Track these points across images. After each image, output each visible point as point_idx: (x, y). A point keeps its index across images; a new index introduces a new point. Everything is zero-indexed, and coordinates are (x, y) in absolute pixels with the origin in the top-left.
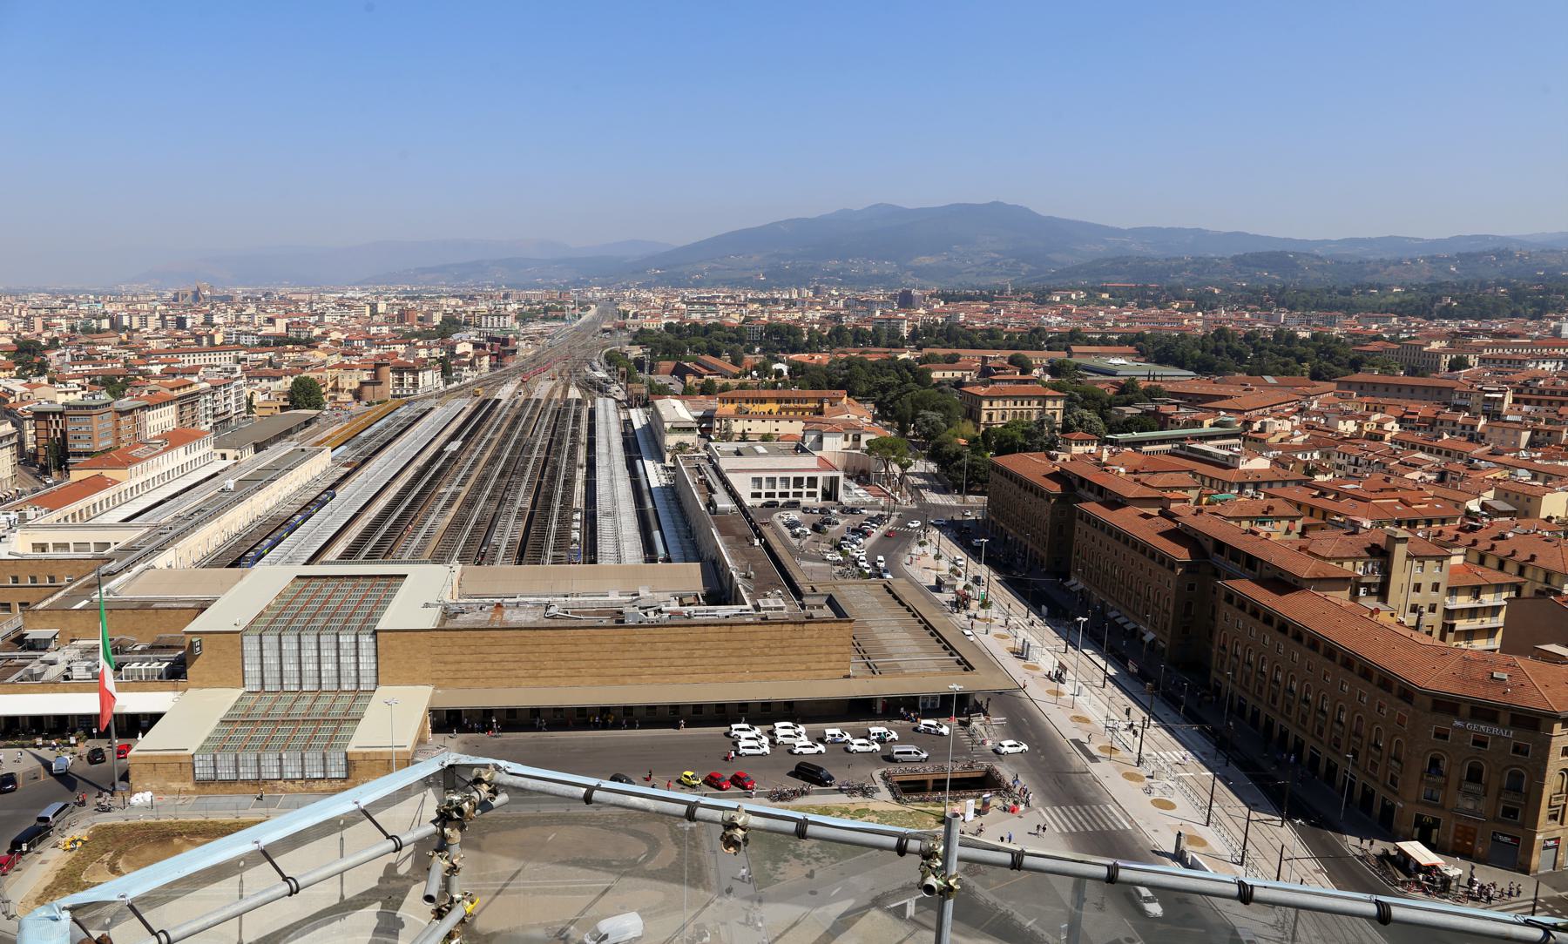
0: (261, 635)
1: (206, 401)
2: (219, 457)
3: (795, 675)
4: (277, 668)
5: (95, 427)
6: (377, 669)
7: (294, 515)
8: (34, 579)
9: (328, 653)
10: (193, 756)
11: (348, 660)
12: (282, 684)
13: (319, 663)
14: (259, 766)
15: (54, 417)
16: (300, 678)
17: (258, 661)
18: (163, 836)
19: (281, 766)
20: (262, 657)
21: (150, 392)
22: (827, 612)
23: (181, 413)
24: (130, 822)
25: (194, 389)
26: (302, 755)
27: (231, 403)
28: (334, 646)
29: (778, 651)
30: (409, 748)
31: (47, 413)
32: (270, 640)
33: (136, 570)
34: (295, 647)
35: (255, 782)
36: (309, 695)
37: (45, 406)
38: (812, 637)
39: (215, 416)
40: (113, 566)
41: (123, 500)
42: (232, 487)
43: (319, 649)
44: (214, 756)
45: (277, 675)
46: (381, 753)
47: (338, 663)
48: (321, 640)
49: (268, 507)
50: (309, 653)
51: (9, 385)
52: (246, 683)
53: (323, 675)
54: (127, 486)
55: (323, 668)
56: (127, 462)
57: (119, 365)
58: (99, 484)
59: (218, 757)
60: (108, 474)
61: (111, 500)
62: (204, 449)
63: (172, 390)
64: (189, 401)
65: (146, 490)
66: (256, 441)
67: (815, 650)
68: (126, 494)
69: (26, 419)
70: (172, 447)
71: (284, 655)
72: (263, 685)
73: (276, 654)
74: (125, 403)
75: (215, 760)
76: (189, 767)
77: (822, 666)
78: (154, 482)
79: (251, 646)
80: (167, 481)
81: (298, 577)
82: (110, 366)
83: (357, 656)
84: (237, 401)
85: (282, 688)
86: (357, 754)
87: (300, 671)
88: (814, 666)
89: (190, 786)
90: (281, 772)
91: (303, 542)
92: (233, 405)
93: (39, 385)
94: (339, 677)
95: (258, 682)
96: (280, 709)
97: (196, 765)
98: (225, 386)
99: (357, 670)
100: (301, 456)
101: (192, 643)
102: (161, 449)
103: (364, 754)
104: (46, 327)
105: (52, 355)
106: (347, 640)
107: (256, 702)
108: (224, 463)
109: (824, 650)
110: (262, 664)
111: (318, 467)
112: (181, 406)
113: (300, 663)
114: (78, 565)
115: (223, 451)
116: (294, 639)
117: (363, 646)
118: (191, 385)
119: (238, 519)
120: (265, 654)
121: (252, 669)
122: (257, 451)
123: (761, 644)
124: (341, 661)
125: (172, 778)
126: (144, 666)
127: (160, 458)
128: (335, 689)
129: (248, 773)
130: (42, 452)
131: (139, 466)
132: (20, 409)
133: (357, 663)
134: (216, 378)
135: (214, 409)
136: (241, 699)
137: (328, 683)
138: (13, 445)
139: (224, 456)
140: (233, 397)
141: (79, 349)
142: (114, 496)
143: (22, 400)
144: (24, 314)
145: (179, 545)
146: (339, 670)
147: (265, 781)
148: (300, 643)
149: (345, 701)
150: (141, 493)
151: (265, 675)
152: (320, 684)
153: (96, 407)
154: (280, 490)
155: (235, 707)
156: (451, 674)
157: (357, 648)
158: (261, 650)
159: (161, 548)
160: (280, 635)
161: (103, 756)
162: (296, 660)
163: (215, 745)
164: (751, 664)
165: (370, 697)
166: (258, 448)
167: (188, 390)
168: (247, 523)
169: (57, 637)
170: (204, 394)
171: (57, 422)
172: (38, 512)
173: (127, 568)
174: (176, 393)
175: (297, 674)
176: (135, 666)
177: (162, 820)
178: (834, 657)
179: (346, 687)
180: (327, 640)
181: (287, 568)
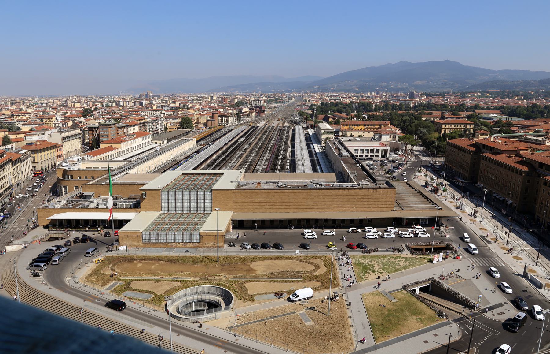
0: (168, 191)
1: (150, 125)
2: (154, 143)
3: (373, 209)
4: (174, 204)
5: (109, 132)
6: (212, 205)
7: (182, 160)
8: (86, 178)
9: (194, 198)
10: (142, 232)
11: (201, 201)
12: (176, 210)
13: (190, 202)
14: (166, 237)
15: (95, 129)
16: (183, 208)
17: (167, 201)
18: (131, 260)
19: (175, 237)
20: (168, 200)
21: (129, 121)
22: (386, 186)
23: (141, 129)
24: (119, 255)
25: (145, 121)
26: (183, 233)
27: (159, 127)
28: (196, 196)
29: (367, 200)
30: (223, 231)
31: (93, 128)
32: (172, 193)
33: (123, 174)
34: (181, 196)
35: (164, 243)
36: (186, 214)
37: (92, 126)
38: (380, 195)
39: (153, 131)
40: (115, 172)
41: (119, 155)
42: (158, 150)
43: (190, 197)
44: (150, 233)
45: (174, 207)
46: (213, 233)
47: (197, 202)
48: (191, 194)
49: (172, 157)
50: (186, 198)
51: (80, 120)
52: (163, 209)
53: (191, 207)
54: (120, 150)
55: (191, 204)
56: (120, 141)
57: (119, 116)
58: (110, 149)
59: (151, 233)
60: (114, 145)
61: (114, 155)
62: (149, 139)
63: (138, 120)
64: (143, 125)
65: (127, 152)
66: (168, 138)
67: (381, 200)
68: (120, 153)
69: (85, 131)
70: (137, 137)
71: (177, 199)
72: (168, 210)
73: (174, 198)
74: (121, 124)
75: (150, 234)
76: (140, 236)
77: (383, 206)
78: (130, 150)
79: (164, 195)
80: (135, 150)
81: (183, 174)
82: (115, 116)
83: (204, 200)
84: (161, 126)
85: (176, 212)
86: (203, 233)
87: (183, 205)
88: (380, 206)
89: (141, 244)
90: (175, 240)
91: (185, 168)
92: (160, 128)
93: (90, 120)
94: (197, 208)
95: (167, 209)
96: (174, 219)
97: (143, 236)
98: (157, 120)
99: (204, 205)
100: (186, 141)
101: (142, 194)
102: (133, 138)
103: (206, 233)
104: (93, 105)
105: (95, 112)
106: (201, 193)
107: (166, 216)
108: (156, 145)
109: (384, 200)
110: (168, 202)
111: (190, 145)
112: (141, 127)
113: (183, 202)
114: (102, 172)
115: (156, 141)
116: (181, 193)
117: (207, 196)
118: (144, 119)
119: (161, 160)
120: (169, 198)
121: (164, 204)
122: (168, 142)
123: (360, 197)
124: (198, 202)
125: (134, 241)
126: (125, 203)
127: (133, 141)
128: (196, 212)
129: (162, 240)
130: (91, 142)
131: (125, 143)
132: (83, 127)
133: (204, 203)
134: (153, 118)
135: (153, 129)
136: (160, 215)
137: (193, 210)
138: (80, 137)
139: (156, 143)
140: (160, 125)
141: (105, 110)
142: (115, 153)
143: (84, 124)
144: (86, 102)
145: (139, 167)
146: (197, 205)
147: (169, 243)
148: (183, 194)
149: (200, 216)
150: (125, 153)
151: (170, 207)
152: (190, 210)
153: (110, 125)
154: (177, 152)
155: (158, 218)
156: (240, 207)
157: (204, 197)
158: (168, 197)
159: (132, 168)
160: (175, 191)
161: (109, 234)
162: (181, 201)
163: (150, 229)
164: (356, 205)
165: (209, 215)
166: (169, 141)
167: (143, 121)
168: (164, 162)
169: (94, 195)
170: (149, 123)
171: (96, 131)
172: (89, 157)
173: (120, 173)
174: (139, 122)
175: (181, 207)
176: (121, 203)
177: (130, 255)
178: (388, 203)
179: (200, 212)
180: (193, 194)
181: (178, 171)
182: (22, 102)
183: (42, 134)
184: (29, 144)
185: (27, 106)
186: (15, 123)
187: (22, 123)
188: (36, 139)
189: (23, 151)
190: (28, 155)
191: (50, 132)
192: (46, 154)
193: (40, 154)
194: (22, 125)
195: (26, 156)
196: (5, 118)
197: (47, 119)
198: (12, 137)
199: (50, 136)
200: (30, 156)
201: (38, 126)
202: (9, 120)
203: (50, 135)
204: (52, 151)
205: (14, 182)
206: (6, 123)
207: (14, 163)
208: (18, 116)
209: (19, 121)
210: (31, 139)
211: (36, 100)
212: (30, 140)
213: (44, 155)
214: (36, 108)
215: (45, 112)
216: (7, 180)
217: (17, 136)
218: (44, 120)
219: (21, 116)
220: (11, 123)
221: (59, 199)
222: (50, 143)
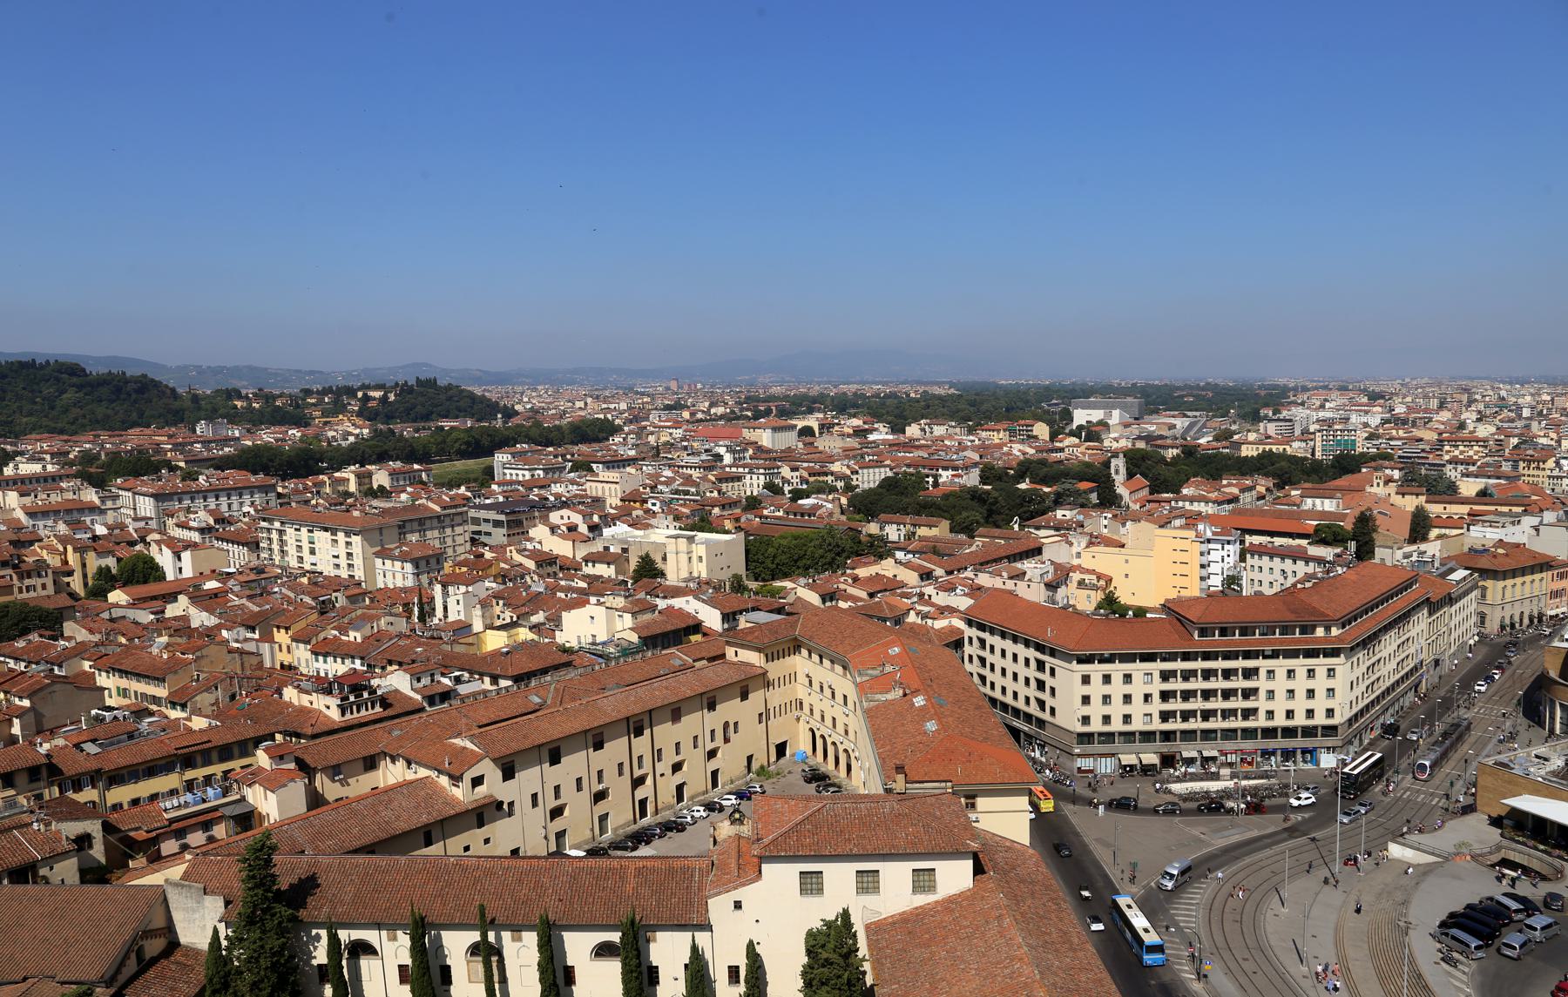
182: (1465, 398)
183: (1513, 523)
184: (1476, 551)
185: (1479, 412)
186: (1444, 465)
187: (1460, 468)
188: (1497, 537)
189: (1460, 574)
190: (1470, 585)
191: (1535, 521)
192: (1519, 585)
193: (1501, 584)
194: (1463, 475)
195: (1466, 587)
196: (1423, 450)
197: (1529, 461)
198: (1435, 509)
199: (1534, 533)
200: (1475, 587)
201: (1502, 481)
202: (1432, 459)
203: (1537, 530)
204: (1537, 576)
205: (1427, 657)
206: (1424, 464)
207: (1433, 606)
208: (1454, 446)
209: (1455, 461)
210: (1483, 535)
211: (1503, 393)
212: (1480, 535)
213: (1514, 586)
214: (1501, 421)
215: (1527, 440)
216: (1412, 650)
217: (1445, 508)
218: (1522, 464)
219: (1461, 448)
220: (1434, 465)
221: (1542, 750)
222: (1534, 555)
